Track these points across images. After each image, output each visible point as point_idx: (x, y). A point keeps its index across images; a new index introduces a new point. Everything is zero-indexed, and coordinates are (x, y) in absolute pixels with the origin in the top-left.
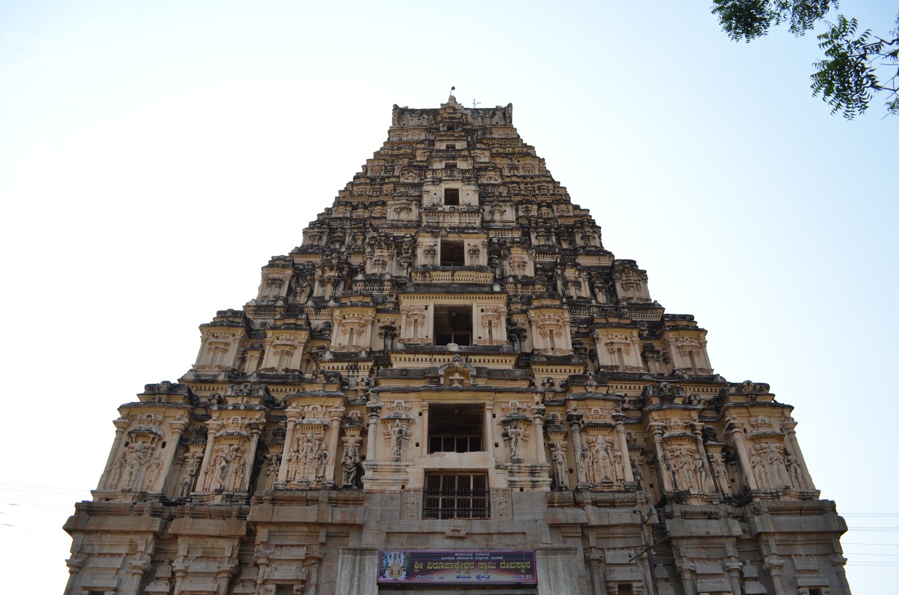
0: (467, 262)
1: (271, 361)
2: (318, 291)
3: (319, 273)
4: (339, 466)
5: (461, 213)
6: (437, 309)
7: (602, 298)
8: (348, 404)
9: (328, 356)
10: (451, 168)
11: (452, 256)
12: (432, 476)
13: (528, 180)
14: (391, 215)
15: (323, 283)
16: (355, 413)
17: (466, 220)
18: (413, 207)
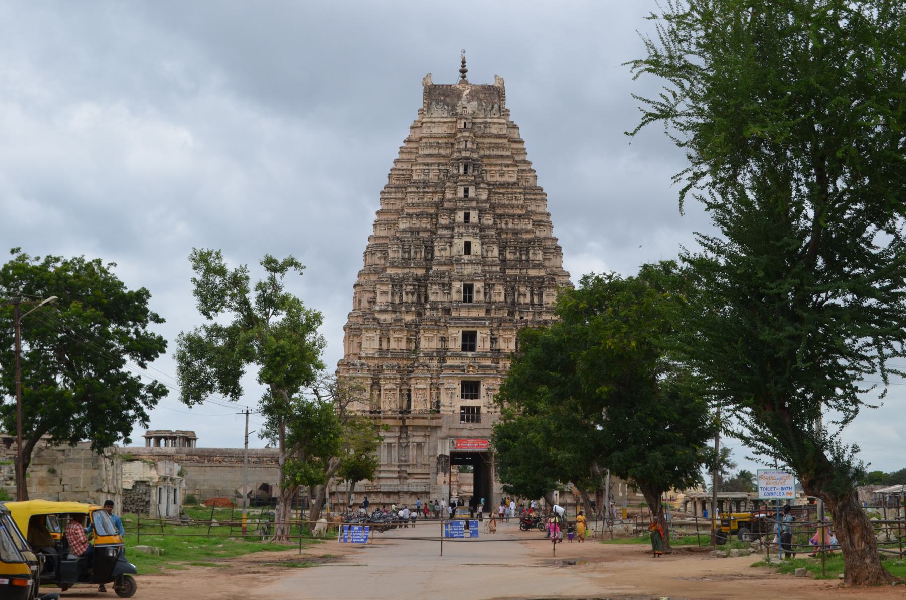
0: (475, 297)
1: (393, 345)
2: (405, 298)
3: (404, 287)
4: (431, 402)
5: (473, 264)
6: (463, 332)
7: (536, 300)
8: (432, 378)
9: (422, 355)
10: (467, 217)
11: (468, 289)
12: (462, 408)
13: (510, 190)
14: (437, 253)
15: (407, 293)
16: (434, 381)
17: (475, 267)
18: (447, 247)
